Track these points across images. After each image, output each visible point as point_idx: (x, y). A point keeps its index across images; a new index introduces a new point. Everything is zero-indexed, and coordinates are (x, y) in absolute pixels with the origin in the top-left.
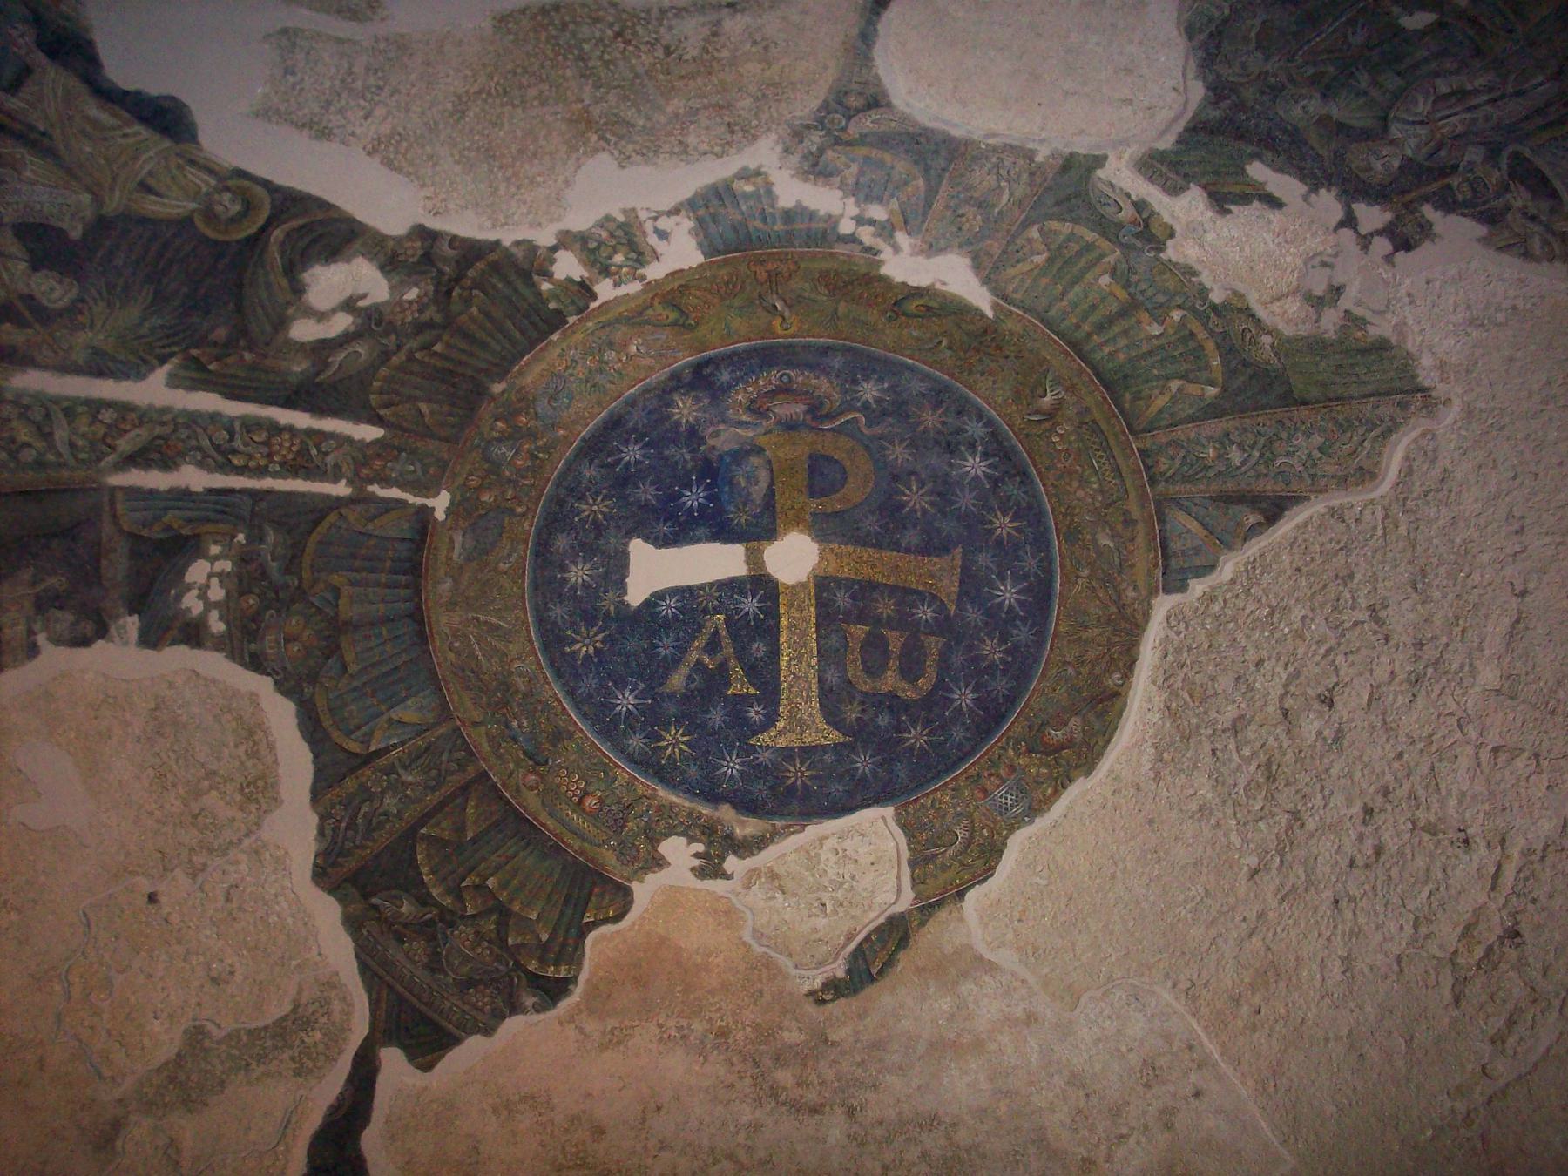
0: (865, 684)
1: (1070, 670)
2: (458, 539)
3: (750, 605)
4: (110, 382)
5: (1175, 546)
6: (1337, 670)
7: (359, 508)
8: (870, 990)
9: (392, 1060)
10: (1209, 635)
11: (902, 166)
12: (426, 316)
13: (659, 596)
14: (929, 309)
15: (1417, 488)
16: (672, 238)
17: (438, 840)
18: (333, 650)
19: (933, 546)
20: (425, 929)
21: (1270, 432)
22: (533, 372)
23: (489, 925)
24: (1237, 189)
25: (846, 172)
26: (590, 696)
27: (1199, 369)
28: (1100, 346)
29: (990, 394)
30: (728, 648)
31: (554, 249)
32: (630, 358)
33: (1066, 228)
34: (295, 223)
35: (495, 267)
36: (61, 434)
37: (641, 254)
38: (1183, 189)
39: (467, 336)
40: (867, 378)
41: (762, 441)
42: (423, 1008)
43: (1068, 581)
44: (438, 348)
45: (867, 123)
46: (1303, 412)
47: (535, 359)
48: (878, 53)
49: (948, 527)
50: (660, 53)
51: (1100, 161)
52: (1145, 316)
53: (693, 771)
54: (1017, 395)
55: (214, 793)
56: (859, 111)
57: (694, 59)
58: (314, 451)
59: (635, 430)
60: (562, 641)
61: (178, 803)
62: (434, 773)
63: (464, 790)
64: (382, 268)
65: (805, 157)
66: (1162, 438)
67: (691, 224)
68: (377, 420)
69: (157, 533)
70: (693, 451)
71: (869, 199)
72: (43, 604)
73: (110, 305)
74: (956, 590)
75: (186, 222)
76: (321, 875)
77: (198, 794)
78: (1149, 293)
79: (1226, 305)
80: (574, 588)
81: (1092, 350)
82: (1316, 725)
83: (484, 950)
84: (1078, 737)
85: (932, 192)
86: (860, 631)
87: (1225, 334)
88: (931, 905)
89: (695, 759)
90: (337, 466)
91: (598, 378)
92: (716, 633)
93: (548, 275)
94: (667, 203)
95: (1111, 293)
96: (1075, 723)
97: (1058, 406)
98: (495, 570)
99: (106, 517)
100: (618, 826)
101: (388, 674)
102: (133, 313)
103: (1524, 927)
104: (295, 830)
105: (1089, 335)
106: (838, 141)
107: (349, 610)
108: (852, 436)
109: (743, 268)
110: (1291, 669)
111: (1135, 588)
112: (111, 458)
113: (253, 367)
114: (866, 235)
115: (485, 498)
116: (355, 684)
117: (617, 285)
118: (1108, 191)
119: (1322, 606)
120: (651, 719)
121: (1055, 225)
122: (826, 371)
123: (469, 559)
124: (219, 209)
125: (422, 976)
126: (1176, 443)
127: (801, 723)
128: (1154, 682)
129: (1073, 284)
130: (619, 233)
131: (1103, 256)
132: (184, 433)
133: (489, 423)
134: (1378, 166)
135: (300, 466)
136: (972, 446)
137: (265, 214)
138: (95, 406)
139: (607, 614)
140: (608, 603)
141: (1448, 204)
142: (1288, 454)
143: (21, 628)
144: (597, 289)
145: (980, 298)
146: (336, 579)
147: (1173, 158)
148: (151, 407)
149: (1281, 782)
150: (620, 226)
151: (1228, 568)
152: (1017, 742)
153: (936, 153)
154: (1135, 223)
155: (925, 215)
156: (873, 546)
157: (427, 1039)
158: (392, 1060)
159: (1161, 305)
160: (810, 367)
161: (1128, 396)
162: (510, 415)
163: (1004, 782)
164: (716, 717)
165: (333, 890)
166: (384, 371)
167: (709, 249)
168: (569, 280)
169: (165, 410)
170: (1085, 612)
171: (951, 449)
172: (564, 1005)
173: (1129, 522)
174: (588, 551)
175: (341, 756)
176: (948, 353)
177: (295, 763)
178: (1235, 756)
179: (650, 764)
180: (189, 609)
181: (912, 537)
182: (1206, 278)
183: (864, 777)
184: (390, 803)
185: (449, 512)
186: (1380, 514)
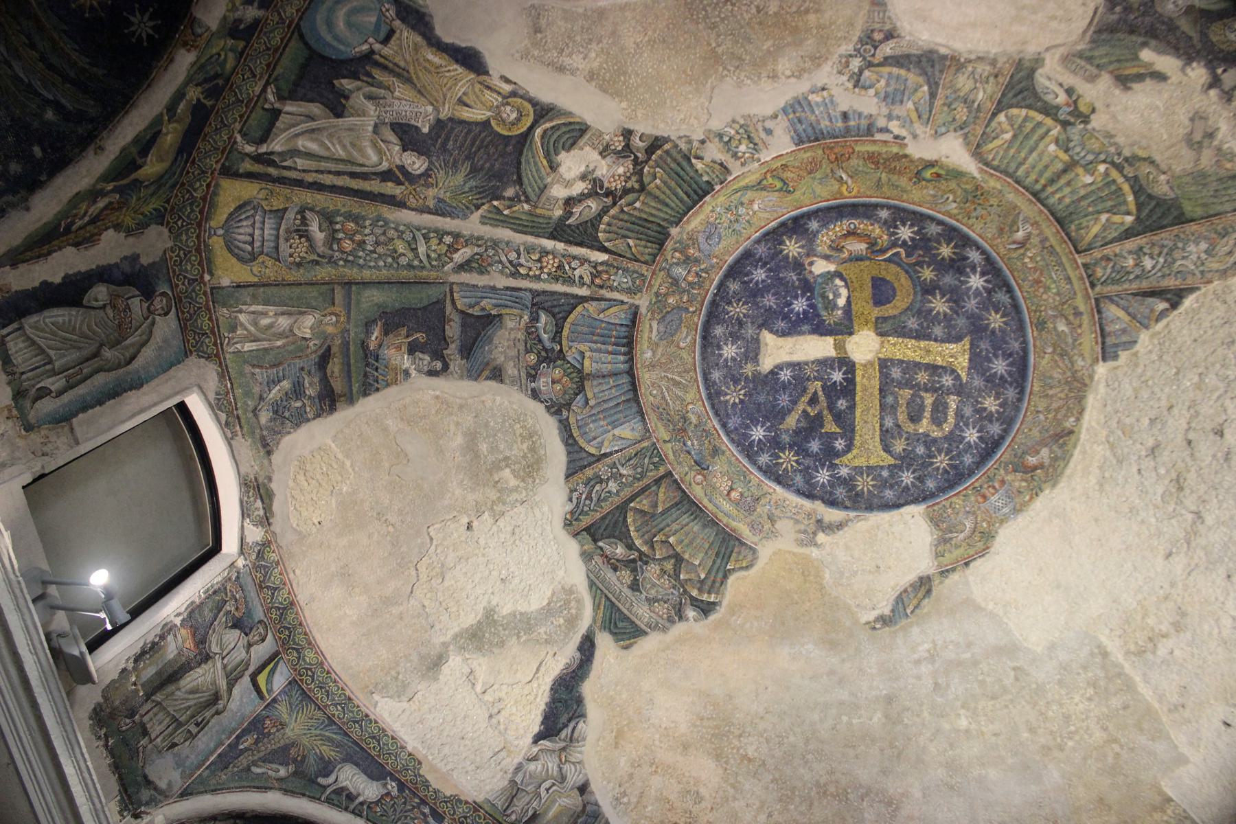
0: (910, 427)
1: (1041, 417)
3: (837, 376)
4: (448, 219)
5: (1107, 329)
6: (1225, 410)
7: (594, 303)
8: (904, 622)
9: (604, 642)
10: (1136, 391)
11: (913, 78)
12: (629, 185)
13: (780, 367)
14: (938, 175)
16: (775, 133)
17: (642, 511)
18: (581, 389)
20: (630, 564)
21: (1171, 244)
22: (695, 221)
23: (669, 566)
24: (1134, 71)
25: (878, 85)
26: (736, 429)
27: (1120, 204)
28: (1053, 193)
31: (703, 142)
32: (755, 213)
33: (1024, 112)
34: (548, 125)
35: (667, 152)
36: (422, 249)
37: (755, 144)
40: (904, 225)
42: (626, 612)
44: (637, 205)
45: (887, 49)
46: (1192, 227)
47: (697, 212)
50: (754, 11)
51: (1038, 61)
52: (1080, 171)
53: (799, 479)
54: (1001, 230)
55: (508, 470)
56: (881, 42)
57: (775, 13)
58: (567, 268)
59: (760, 259)
60: (719, 393)
63: (658, 481)
64: (601, 153)
65: (851, 77)
66: (1097, 254)
67: (787, 124)
68: (605, 250)
69: (476, 312)
70: (799, 274)
72: (413, 349)
73: (447, 173)
74: (966, 364)
75: (486, 124)
76: (567, 524)
78: (1082, 154)
80: (726, 360)
81: (1047, 197)
83: (665, 581)
84: (1047, 461)
85: (933, 95)
86: (907, 393)
87: (1136, 178)
88: (947, 571)
89: (800, 471)
90: (581, 277)
91: (736, 226)
92: (815, 393)
94: (769, 111)
95: (1057, 157)
96: (1045, 452)
97: (1028, 237)
98: (678, 346)
100: (750, 510)
101: (612, 408)
102: (459, 178)
104: (554, 497)
105: (1045, 186)
106: (870, 65)
108: (899, 265)
109: (820, 152)
110: (1192, 411)
111: (1084, 359)
112: (451, 265)
113: (530, 213)
114: (894, 126)
115: (670, 301)
116: (593, 412)
117: (743, 165)
118: (1047, 83)
119: (1213, 364)
120: (775, 444)
121: (1015, 111)
122: (878, 220)
123: (661, 339)
124: (505, 116)
125: (628, 592)
126: (1107, 259)
127: (867, 452)
129: (1031, 151)
130: (741, 131)
131: (1049, 130)
132: (491, 252)
133: (670, 252)
135: (560, 275)
136: (974, 269)
138: (441, 234)
139: (747, 378)
142: (1184, 258)
144: (730, 166)
145: (969, 165)
146: (582, 347)
147: (1088, 54)
148: (472, 236)
149: (1187, 491)
150: (741, 127)
152: (1006, 465)
154: (1068, 105)
155: (930, 111)
156: (915, 338)
157: (626, 630)
158: (604, 642)
159: (1091, 162)
161: (1073, 227)
163: (997, 491)
164: (815, 446)
165: (575, 535)
166: (606, 219)
167: (800, 142)
168: (714, 162)
169: (478, 239)
170: (1051, 377)
171: (961, 271)
172: (713, 617)
173: (1078, 314)
174: (735, 337)
175: (584, 455)
176: (954, 205)
179: (772, 473)
180: (495, 359)
181: (938, 331)
182: (1120, 140)
183: (907, 488)
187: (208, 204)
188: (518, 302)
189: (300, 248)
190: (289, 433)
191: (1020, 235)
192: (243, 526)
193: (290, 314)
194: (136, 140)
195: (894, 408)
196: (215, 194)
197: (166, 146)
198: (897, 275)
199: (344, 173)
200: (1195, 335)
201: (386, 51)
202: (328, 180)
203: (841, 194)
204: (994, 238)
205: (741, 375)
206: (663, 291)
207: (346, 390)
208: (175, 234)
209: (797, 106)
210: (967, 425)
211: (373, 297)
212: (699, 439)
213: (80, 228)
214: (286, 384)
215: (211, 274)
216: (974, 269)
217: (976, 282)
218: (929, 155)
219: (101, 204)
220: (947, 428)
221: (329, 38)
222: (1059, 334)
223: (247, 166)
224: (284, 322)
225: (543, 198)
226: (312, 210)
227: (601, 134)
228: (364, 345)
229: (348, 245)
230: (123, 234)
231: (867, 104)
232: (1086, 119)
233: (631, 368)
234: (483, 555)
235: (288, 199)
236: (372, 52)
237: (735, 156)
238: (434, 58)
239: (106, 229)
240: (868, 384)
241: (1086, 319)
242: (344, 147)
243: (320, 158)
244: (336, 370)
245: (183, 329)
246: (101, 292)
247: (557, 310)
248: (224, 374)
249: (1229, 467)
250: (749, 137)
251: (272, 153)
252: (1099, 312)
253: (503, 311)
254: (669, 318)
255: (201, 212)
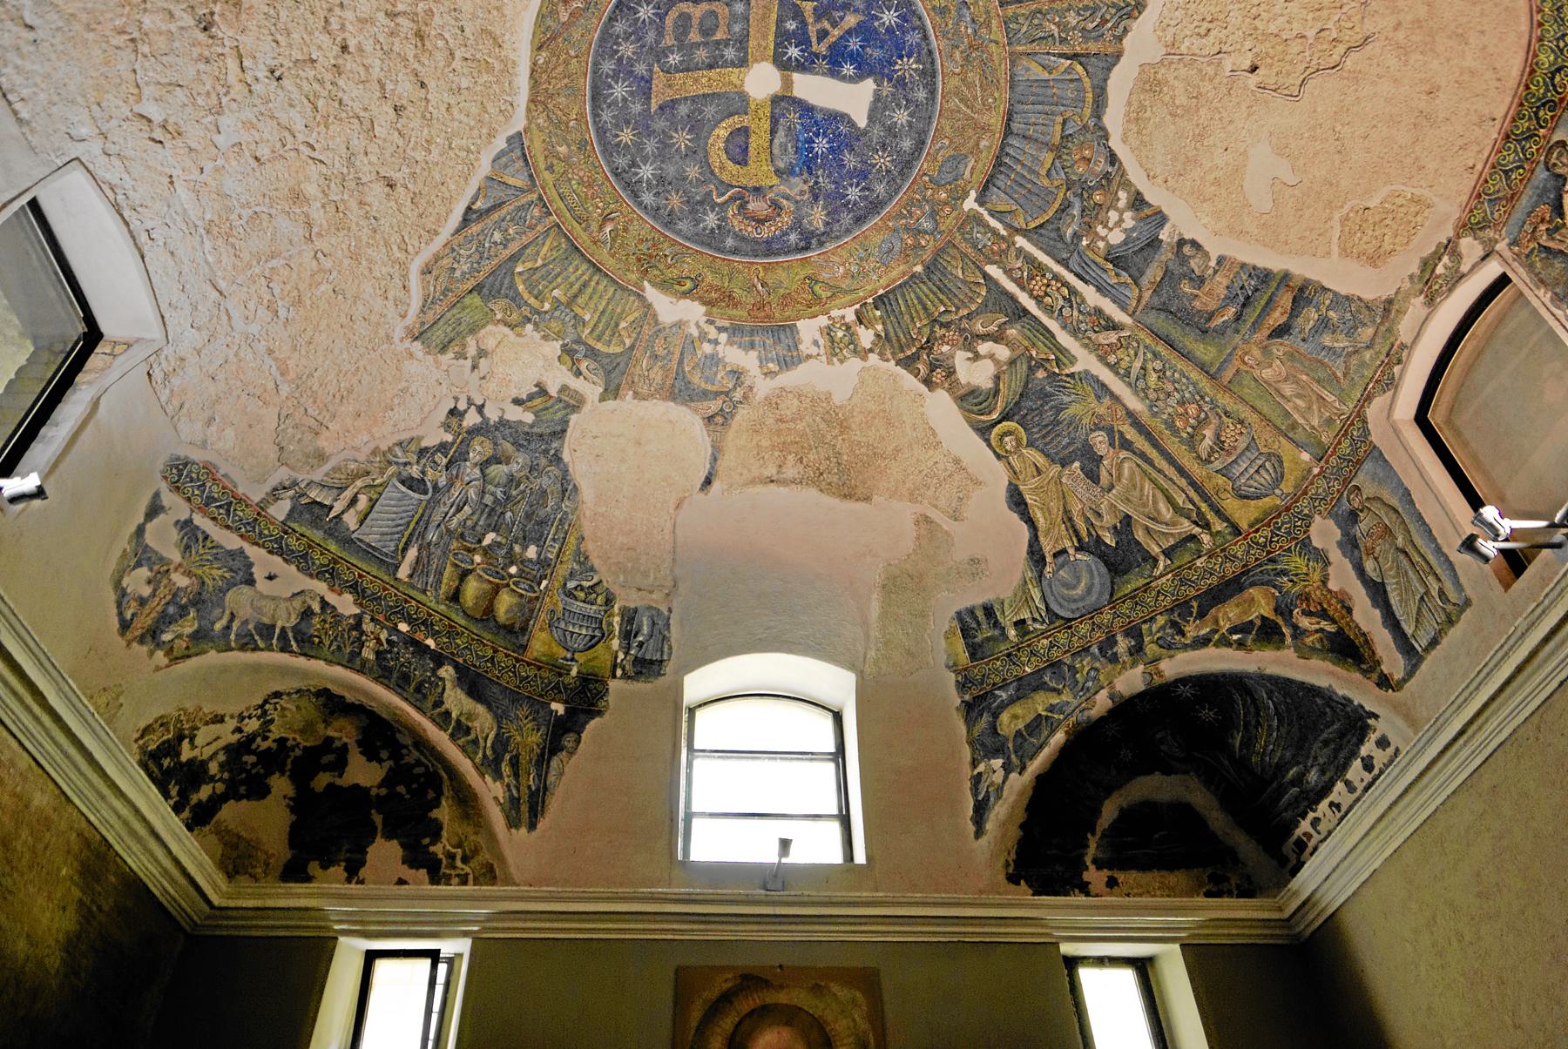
2: (967, 173)
3: (794, 52)
5: (521, 163)
7: (1016, 224)
11: (696, 379)
12: (943, 331)
14: (679, 284)
15: (396, 280)
19: (668, 107)
22: (897, 273)
24: (538, 401)
26: (914, 29)
29: (643, 227)
30: (812, 31)
31: (871, 350)
36: (1137, 364)
38: (560, 391)
39: (925, 308)
40: (712, 230)
41: (775, 180)
43: (581, 117)
44: (942, 309)
45: (714, 406)
46: (469, 285)
47: (894, 281)
48: (710, 450)
49: (660, 124)
51: (602, 399)
52: (563, 299)
54: (625, 230)
60: (923, 73)
61: (1203, 111)
62: (1036, 22)
67: (801, 347)
68: (986, 276)
69: (1125, 277)
70: (816, 183)
71: (713, 356)
75: (1030, 444)
77: (1187, 110)
79: (522, 324)
80: (907, 108)
82: (400, 90)
85: (681, 362)
86: (719, 35)
93: (878, 336)
97: (601, 228)
99: (1143, 302)
103: (202, 37)
106: (727, 394)
107: (1048, 158)
114: (712, 333)
121: (618, 350)
122: (736, 235)
126: (532, 227)
128: (514, 63)
129: (603, 312)
134: (478, 448)
137: (996, 430)
138: (1113, 368)
139: (890, 80)
140: (887, 88)
141: (443, 447)
143: (1218, 278)
145: (651, 293)
146: (1046, 182)
151: (484, 167)
153: (680, 391)
160: (743, 239)
162: (917, 247)
167: (793, 328)
169: (1086, 346)
171: (661, 180)
173: (550, 168)
174: (891, 130)
177: (1120, 82)
178: (447, 36)
181: (683, 110)
182: (537, 336)
184: (1072, 19)
185: (966, 194)
186: (410, 248)
187: (1267, 519)
188: (1084, 263)
189: (1229, 435)
190: (1360, 299)
191: (608, 229)
192: (1474, 267)
193: (1277, 391)
194: (1241, 645)
195: (734, 18)
196: (1257, 521)
197: (1237, 611)
198: (722, 168)
199: (1154, 467)
200: (443, 189)
201: (1068, 544)
202: (1171, 472)
203: (765, 269)
204: (631, 220)
205: (894, 86)
206: (947, 209)
207: (1283, 289)
208: (1307, 520)
209: (789, 362)
210: (652, 22)
211: (1205, 351)
212: (956, 32)
213: (1334, 621)
214: (1327, 340)
215: (1310, 471)
216: (649, 182)
217: (646, 172)
218: (686, 303)
219: (1305, 623)
220: (673, 15)
221: (1097, 581)
222: (565, 140)
223: (1219, 526)
224: (1288, 389)
225: (1018, 352)
226: (1199, 457)
227: (948, 390)
228: (1238, 317)
229: (1192, 410)
230: (1330, 570)
231: (734, 356)
232: (567, 350)
233: (1006, 136)
234: (1256, 29)
235: (1210, 478)
236: (1077, 549)
237: (848, 328)
238: (1039, 517)
239: (1330, 591)
240: (763, 39)
241: (542, 166)
242: (1142, 490)
243: (1163, 491)
244: (1277, 314)
245: (1360, 462)
246: (1369, 565)
247: (1053, 235)
248: (1368, 399)
249: (379, 81)
250: (833, 342)
251: (1195, 523)
252: (531, 176)
253: (1100, 261)
254: (949, 178)
255: (1279, 515)
